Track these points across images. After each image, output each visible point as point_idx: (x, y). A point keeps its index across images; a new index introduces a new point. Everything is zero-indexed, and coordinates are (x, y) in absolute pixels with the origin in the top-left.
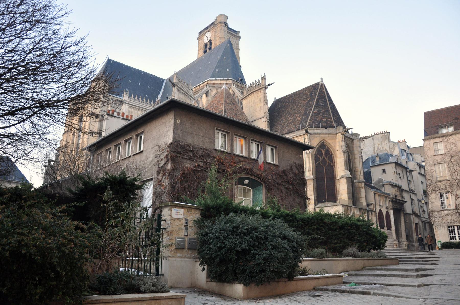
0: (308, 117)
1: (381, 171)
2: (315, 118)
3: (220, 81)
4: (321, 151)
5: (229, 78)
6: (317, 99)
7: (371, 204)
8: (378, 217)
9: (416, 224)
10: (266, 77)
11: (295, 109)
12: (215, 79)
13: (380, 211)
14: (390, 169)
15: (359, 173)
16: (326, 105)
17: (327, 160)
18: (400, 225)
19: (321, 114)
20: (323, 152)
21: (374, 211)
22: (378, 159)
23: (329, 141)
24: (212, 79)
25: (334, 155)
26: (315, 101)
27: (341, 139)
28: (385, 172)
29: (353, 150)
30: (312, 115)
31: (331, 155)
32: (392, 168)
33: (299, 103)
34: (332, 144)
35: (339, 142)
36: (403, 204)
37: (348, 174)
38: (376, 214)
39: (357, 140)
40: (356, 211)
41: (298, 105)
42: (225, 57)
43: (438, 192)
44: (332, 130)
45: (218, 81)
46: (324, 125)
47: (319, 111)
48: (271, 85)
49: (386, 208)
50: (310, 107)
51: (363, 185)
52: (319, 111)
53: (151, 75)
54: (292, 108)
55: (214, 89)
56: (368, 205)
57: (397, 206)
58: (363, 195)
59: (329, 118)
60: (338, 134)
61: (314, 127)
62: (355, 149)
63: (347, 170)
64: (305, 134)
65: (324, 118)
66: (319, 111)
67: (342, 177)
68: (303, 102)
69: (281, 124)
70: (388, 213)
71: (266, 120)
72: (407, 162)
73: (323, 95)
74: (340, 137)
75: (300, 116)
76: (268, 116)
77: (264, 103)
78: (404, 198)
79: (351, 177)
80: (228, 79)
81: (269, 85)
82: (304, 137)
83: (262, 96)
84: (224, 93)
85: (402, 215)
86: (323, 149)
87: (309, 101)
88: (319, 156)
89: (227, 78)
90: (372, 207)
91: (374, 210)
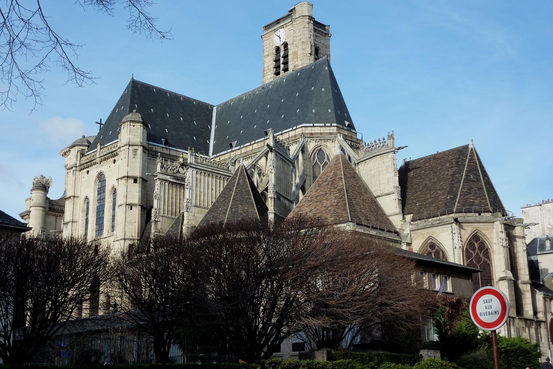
0: (455, 197)
2: (465, 199)
3: (319, 128)
4: (474, 244)
5: (333, 125)
6: (466, 171)
10: (395, 136)
11: (435, 182)
12: (312, 125)
16: (479, 180)
17: (481, 255)
19: (473, 193)
20: (476, 245)
23: (484, 232)
25: (491, 250)
30: (461, 195)
31: (487, 249)
33: (440, 173)
34: (488, 236)
35: (497, 233)
37: (510, 275)
42: (323, 90)
45: (316, 128)
46: (477, 208)
47: (469, 189)
50: (457, 182)
52: (469, 189)
54: (431, 179)
55: (312, 141)
64: (453, 223)
65: (476, 199)
66: (470, 189)
67: (502, 279)
68: (447, 173)
71: (397, 197)
73: (474, 165)
75: (444, 194)
77: (393, 174)
80: (331, 126)
81: (399, 148)
82: (452, 227)
83: (390, 163)
86: (477, 242)
87: (455, 173)
88: (471, 251)
89: (329, 125)
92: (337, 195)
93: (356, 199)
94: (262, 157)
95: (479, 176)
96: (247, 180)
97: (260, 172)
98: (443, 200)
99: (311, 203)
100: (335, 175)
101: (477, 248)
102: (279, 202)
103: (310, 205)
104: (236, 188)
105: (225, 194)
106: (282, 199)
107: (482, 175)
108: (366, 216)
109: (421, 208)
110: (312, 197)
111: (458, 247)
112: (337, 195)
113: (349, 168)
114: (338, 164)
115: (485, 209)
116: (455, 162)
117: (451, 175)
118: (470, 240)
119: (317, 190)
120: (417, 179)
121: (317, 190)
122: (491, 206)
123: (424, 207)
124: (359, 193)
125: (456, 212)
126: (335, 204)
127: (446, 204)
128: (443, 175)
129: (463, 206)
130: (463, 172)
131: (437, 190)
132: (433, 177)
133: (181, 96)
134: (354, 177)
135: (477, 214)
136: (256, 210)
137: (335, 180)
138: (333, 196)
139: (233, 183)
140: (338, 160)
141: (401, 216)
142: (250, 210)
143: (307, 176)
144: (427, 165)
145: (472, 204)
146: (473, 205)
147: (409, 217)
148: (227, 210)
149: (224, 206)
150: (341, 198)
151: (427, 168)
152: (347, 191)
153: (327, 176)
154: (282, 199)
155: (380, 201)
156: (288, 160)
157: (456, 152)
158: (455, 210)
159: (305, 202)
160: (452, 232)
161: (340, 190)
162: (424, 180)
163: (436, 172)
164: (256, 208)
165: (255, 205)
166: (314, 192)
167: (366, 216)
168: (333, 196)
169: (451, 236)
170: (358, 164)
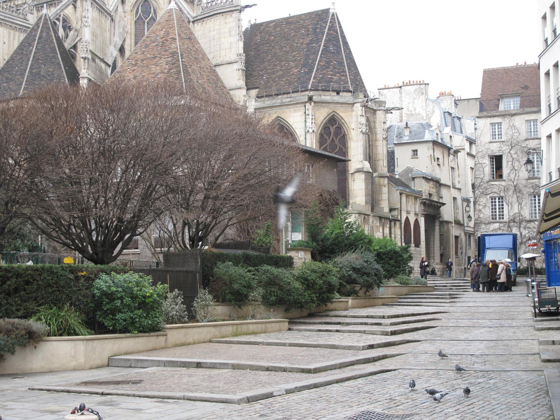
0: (311, 71)
1: (411, 153)
7: (395, 209)
9: (457, 237)
13: (407, 219)
14: (425, 151)
15: (381, 163)
16: (339, 52)
17: (337, 142)
18: (432, 240)
20: (332, 130)
21: (399, 221)
22: (407, 132)
23: (342, 115)
26: (322, 44)
27: (360, 113)
28: (417, 154)
29: (375, 127)
30: (317, 69)
32: (429, 149)
33: (294, 41)
34: (346, 119)
35: (357, 116)
36: (440, 207)
37: (367, 166)
38: (401, 224)
39: (381, 112)
41: (293, 46)
43: (488, 197)
44: (346, 97)
46: (336, 86)
48: (251, 6)
49: (416, 214)
51: (386, 181)
54: (282, 48)
56: (391, 210)
57: (431, 211)
58: (385, 196)
59: (343, 76)
60: (355, 105)
61: (321, 90)
62: (377, 125)
63: (366, 160)
64: (306, 102)
65: (335, 76)
67: (359, 171)
68: (301, 41)
69: (263, 76)
72: (451, 137)
74: (358, 109)
75: (296, 66)
76: (243, 61)
78: (442, 198)
81: (247, 6)
82: (305, 106)
83: (234, 23)
84: (175, 18)
85: (437, 224)
87: (311, 42)
88: (326, 137)
90: (395, 213)
92: (169, 59)
93: (192, 66)
94: (68, 5)
96: (53, 34)
97: (65, 24)
98: (296, 74)
99: (136, 68)
100: (167, 33)
101: (332, 133)
102: (94, 64)
103: (134, 70)
104: (38, 44)
105: (22, 50)
106: (97, 60)
108: (203, 88)
109: (269, 82)
110: (136, 60)
111: (311, 131)
112: (169, 59)
113: (184, 27)
114: (171, 20)
115: (344, 87)
116: (312, 28)
117: (307, 44)
118: (326, 124)
119: (144, 52)
120: (265, 47)
121: (144, 52)
122: (352, 85)
123: (272, 81)
124: (196, 59)
125: (311, 90)
126: (166, 71)
127: (299, 79)
128: (297, 43)
129: (319, 82)
130: (321, 41)
131: (289, 61)
132: (284, 45)
134: (190, 38)
135: (335, 94)
136: (64, 73)
137: (167, 41)
138: (163, 61)
139: (34, 36)
140: (171, 16)
141: (244, 91)
142: (56, 73)
143: (127, 33)
144: (278, 29)
145: (330, 81)
146: (331, 82)
147: (254, 92)
148: (26, 70)
149: (22, 66)
150: (173, 64)
151: (278, 34)
152: (182, 55)
153: (157, 35)
154: (97, 60)
155: (219, 70)
156: (106, 12)
157: (314, 16)
158: (309, 88)
159: (128, 66)
160: (305, 113)
161: (174, 54)
162: (273, 47)
163: (289, 40)
164: (64, 71)
165: (62, 66)
166: (140, 55)
167: (203, 88)
168: (163, 61)
169: (303, 117)
170: (193, 22)
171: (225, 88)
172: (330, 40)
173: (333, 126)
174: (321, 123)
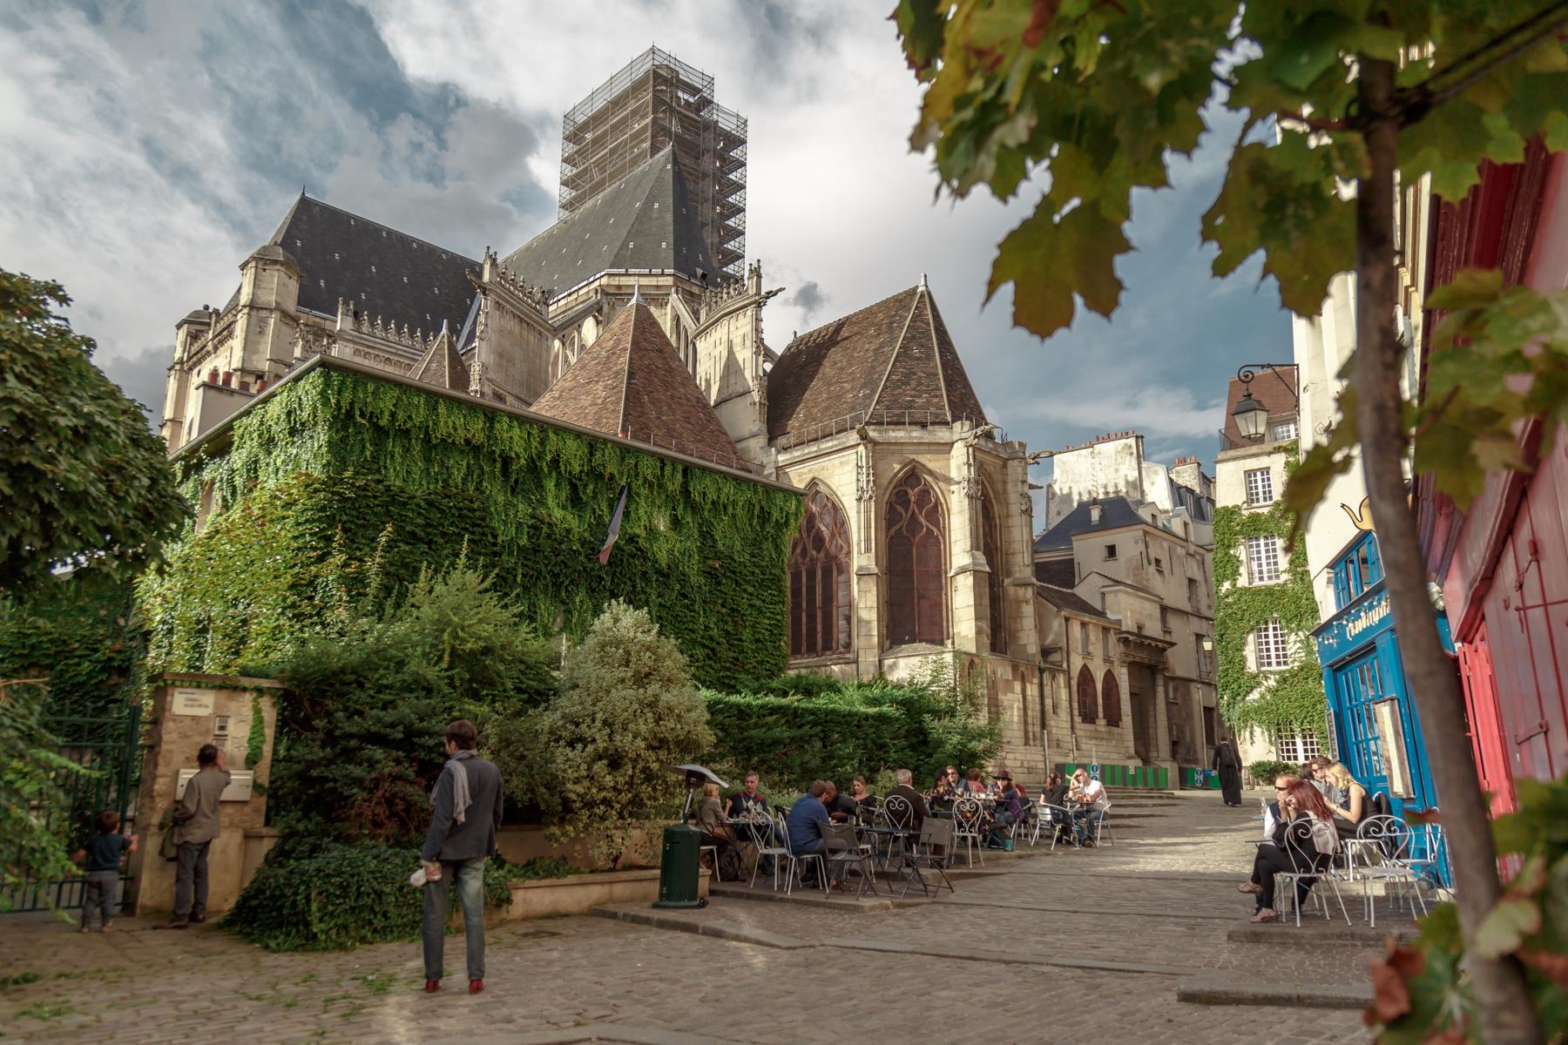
0: (874, 392)
8: (1075, 689)
15: (1019, 558)
16: (930, 357)
18: (1152, 713)
19: (913, 383)
21: (1064, 671)
24: (615, 271)
29: (1005, 492)
31: (936, 506)
32: (1136, 542)
36: (1164, 650)
38: (1070, 678)
39: (1016, 462)
40: (1000, 671)
46: (918, 415)
48: (776, 294)
51: (1029, 593)
53: (444, 251)
57: (1142, 656)
61: (888, 424)
62: (1010, 487)
63: (978, 549)
65: (920, 396)
66: (909, 375)
67: (963, 570)
70: (1110, 678)
75: (852, 389)
78: (1170, 633)
79: (987, 569)
81: (770, 294)
85: (1160, 682)
88: (899, 508)
90: (1055, 657)
91: (1065, 665)
95: (933, 348)
107: (939, 349)
115: (937, 416)
133: (414, 240)
171: (725, 434)
172: (914, 337)
173: (913, 489)
174: (890, 483)
